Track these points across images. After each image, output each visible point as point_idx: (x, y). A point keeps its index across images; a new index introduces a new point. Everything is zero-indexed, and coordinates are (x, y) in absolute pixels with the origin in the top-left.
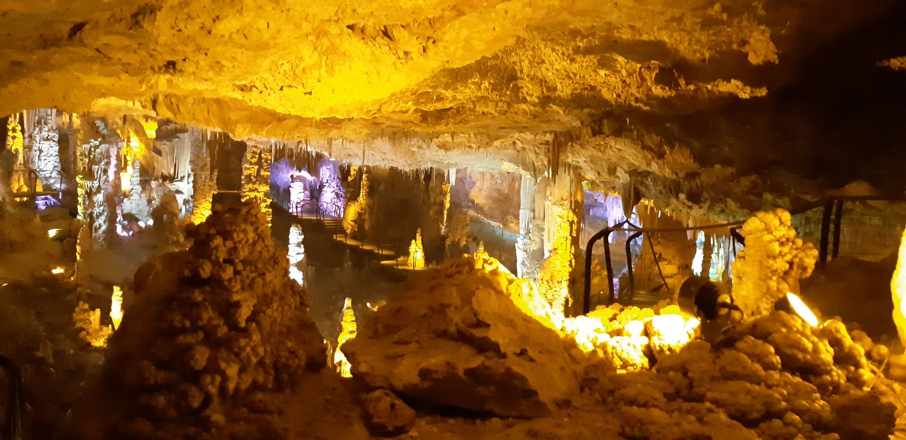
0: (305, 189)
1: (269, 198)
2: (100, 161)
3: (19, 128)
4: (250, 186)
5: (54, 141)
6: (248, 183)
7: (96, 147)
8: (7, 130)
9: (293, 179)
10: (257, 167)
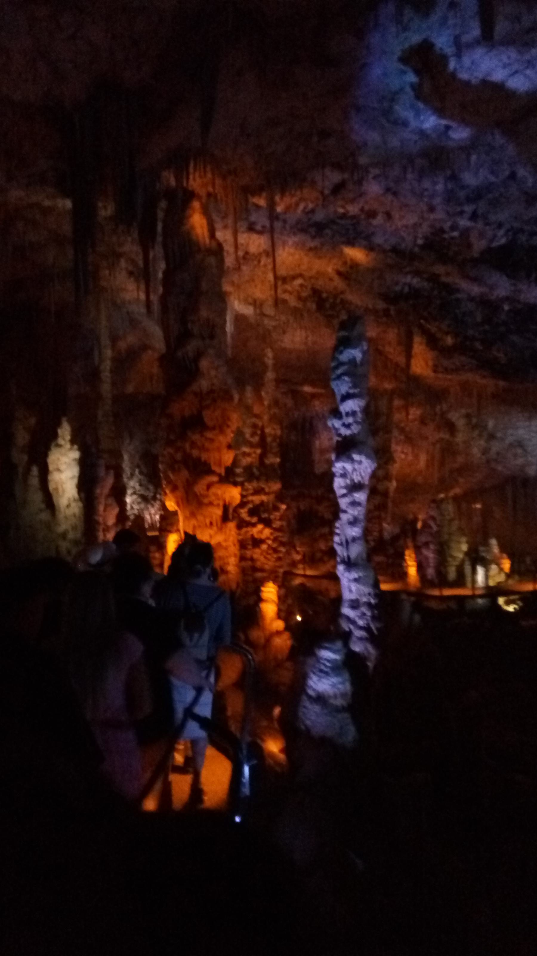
4: (255, 484)
10: (259, 451)
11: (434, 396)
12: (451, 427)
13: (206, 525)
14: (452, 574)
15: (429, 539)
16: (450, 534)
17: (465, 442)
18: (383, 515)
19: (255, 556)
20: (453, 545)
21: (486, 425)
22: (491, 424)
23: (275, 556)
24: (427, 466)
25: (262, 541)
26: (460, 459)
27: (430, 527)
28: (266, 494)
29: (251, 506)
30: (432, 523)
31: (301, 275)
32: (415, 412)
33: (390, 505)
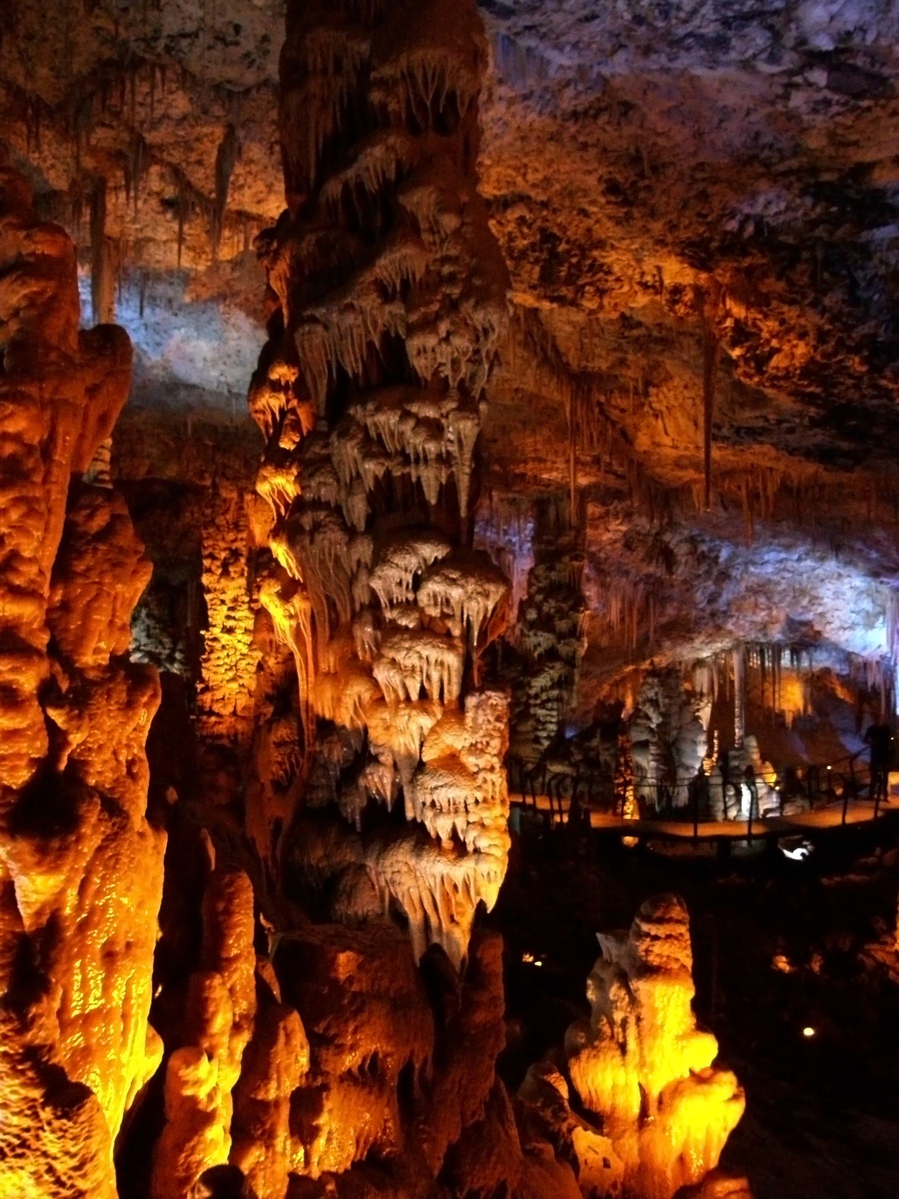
11: (664, 498)
12: (668, 558)
13: (408, 698)
14: (683, 796)
15: (644, 737)
16: (680, 728)
17: (685, 582)
18: (565, 695)
20: (686, 747)
21: (717, 557)
22: (724, 554)
24: (622, 619)
26: (670, 611)
27: (649, 718)
30: (651, 712)
31: (522, 199)
32: (617, 528)
33: (577, 678)
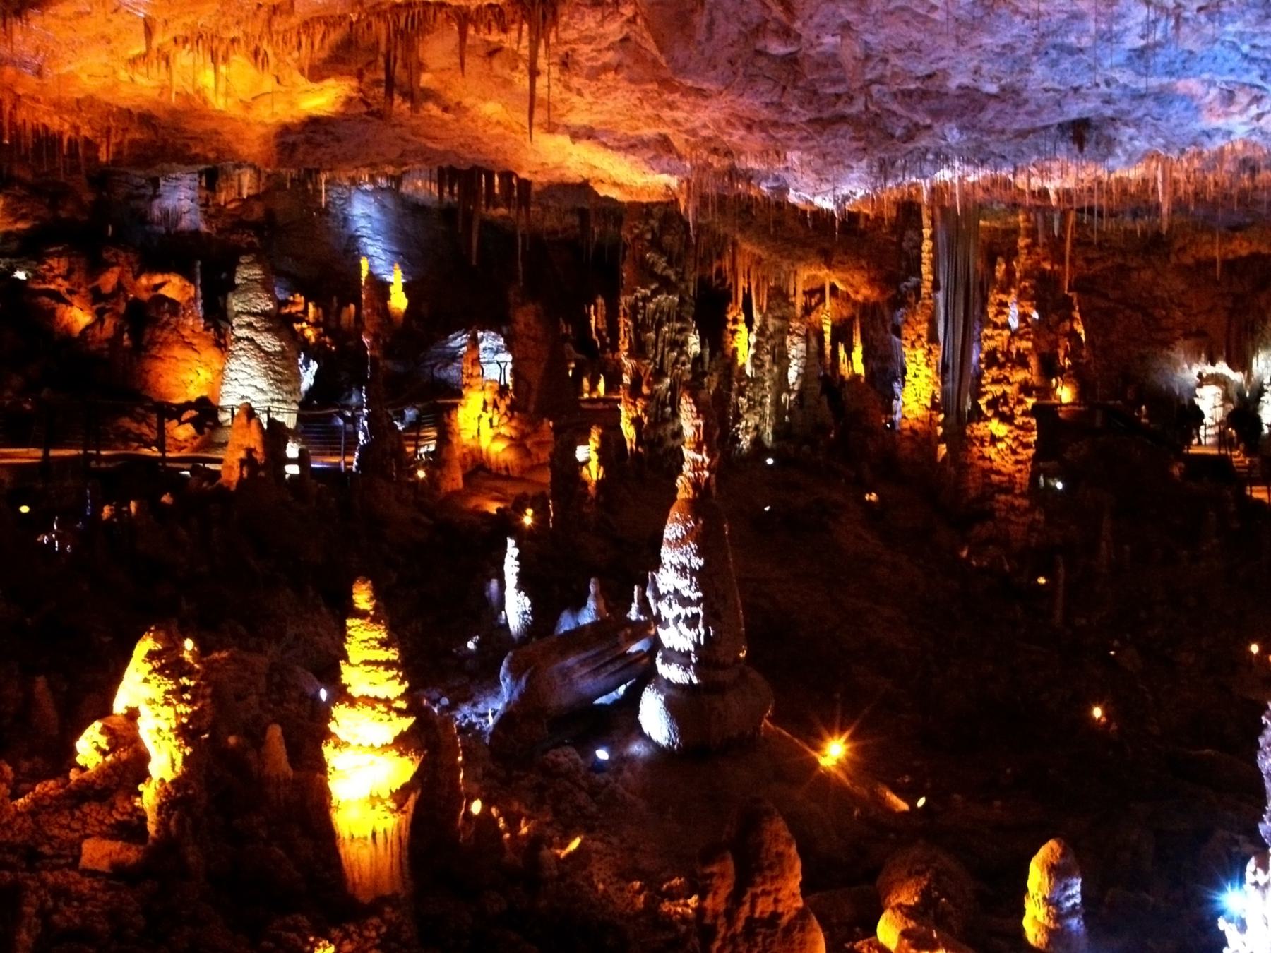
0: (1226, 398)
1: (1029, 395)
2: (659, 325)
3: (742, 317)
4: (994, 372)
5: (799, 335)
6: (989, 367)
7: (646, 299)
8: (727, 321)
9: (1203, 380)
19: (993, 456)
23: (1013, 458)
25: (1001, 440)
28: (1010, 383)
29: (989, 397)
